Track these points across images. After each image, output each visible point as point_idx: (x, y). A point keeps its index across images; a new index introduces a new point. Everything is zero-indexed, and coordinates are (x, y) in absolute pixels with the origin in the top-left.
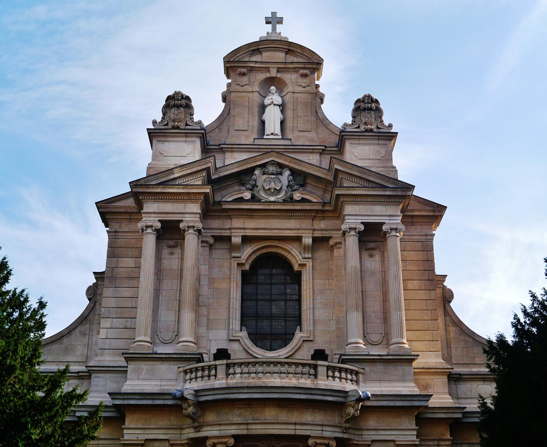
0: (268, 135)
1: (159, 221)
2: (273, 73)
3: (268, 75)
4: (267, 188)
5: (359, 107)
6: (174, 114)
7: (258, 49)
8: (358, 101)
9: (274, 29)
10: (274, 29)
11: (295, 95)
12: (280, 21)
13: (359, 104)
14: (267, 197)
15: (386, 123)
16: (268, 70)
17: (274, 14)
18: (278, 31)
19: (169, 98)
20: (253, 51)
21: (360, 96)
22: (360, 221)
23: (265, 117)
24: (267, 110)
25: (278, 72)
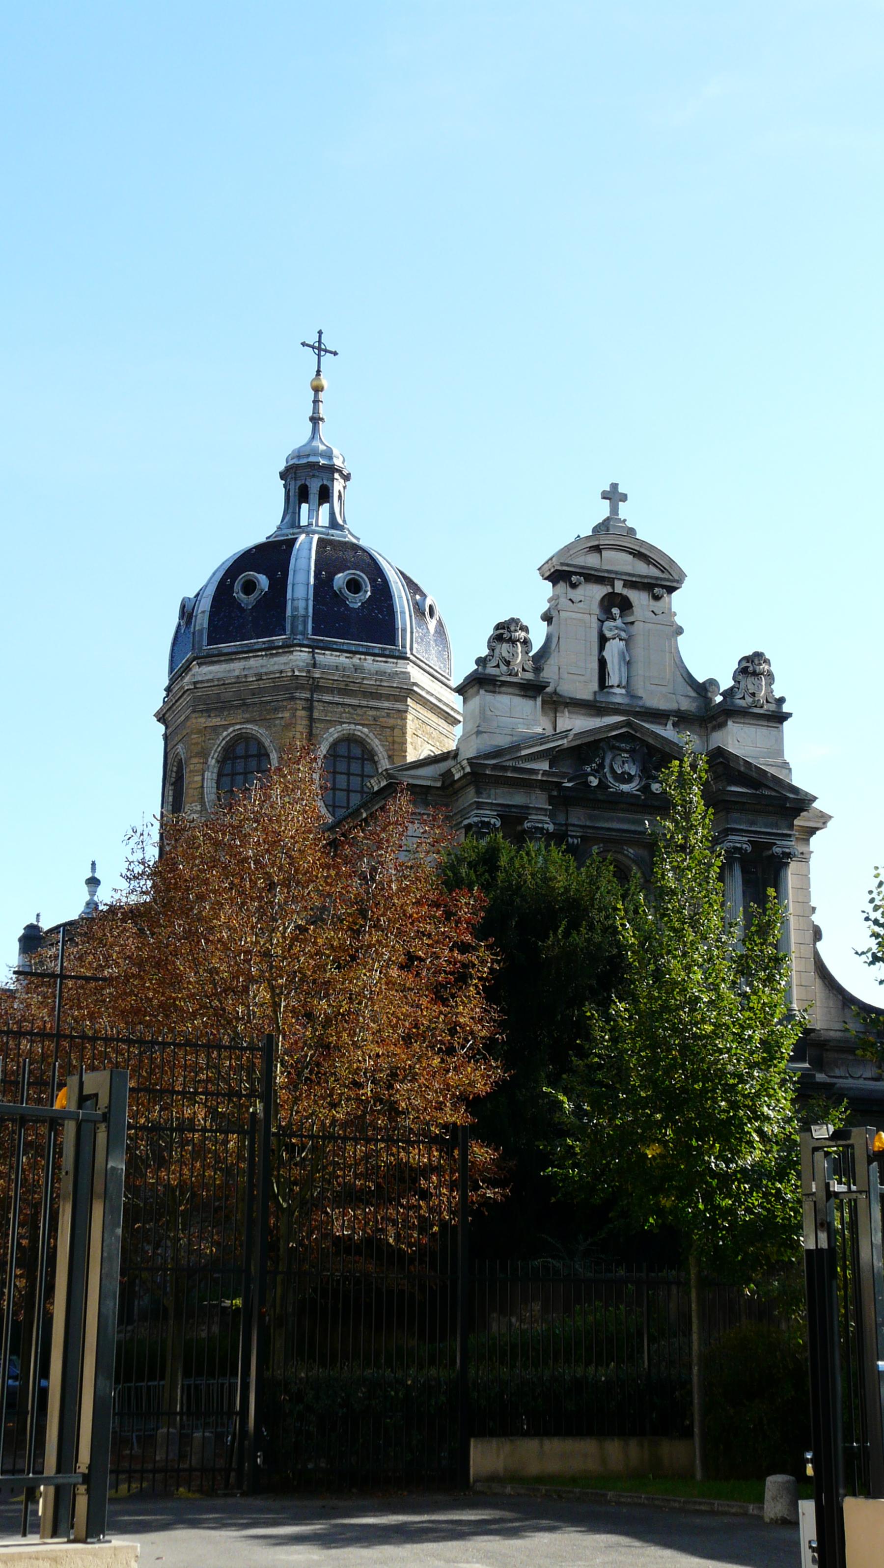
0: (612, 687)
1: (498, 815)
2: (619, 587)
3: (610, 590)
4: (619, 772)
5: (747, 667)
6: (509, 652)
7: (598, 546)
8: (746, 659)
9: (614, 510)
10: (614, 510)
11: (647, 625)
12: (624, 498)
13: (744, 664)
14: (617, 785)
15: (777, 695)
16: (611, 582)
17: (614, 486)
18: (621, 516)
19: (499, 627)
20: (590, 547)
21: (749, 653)
22: (746, 839)
23: (605, 654)
24: (607, 644)
25: (624, 586)
